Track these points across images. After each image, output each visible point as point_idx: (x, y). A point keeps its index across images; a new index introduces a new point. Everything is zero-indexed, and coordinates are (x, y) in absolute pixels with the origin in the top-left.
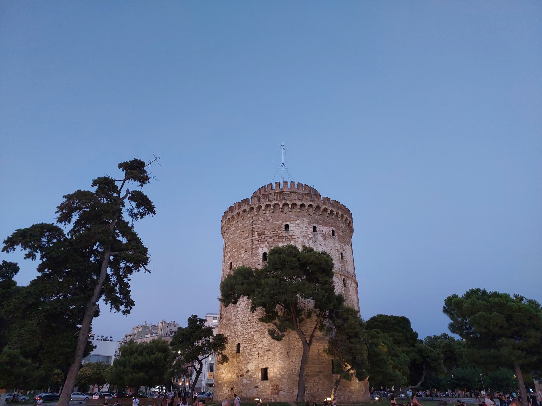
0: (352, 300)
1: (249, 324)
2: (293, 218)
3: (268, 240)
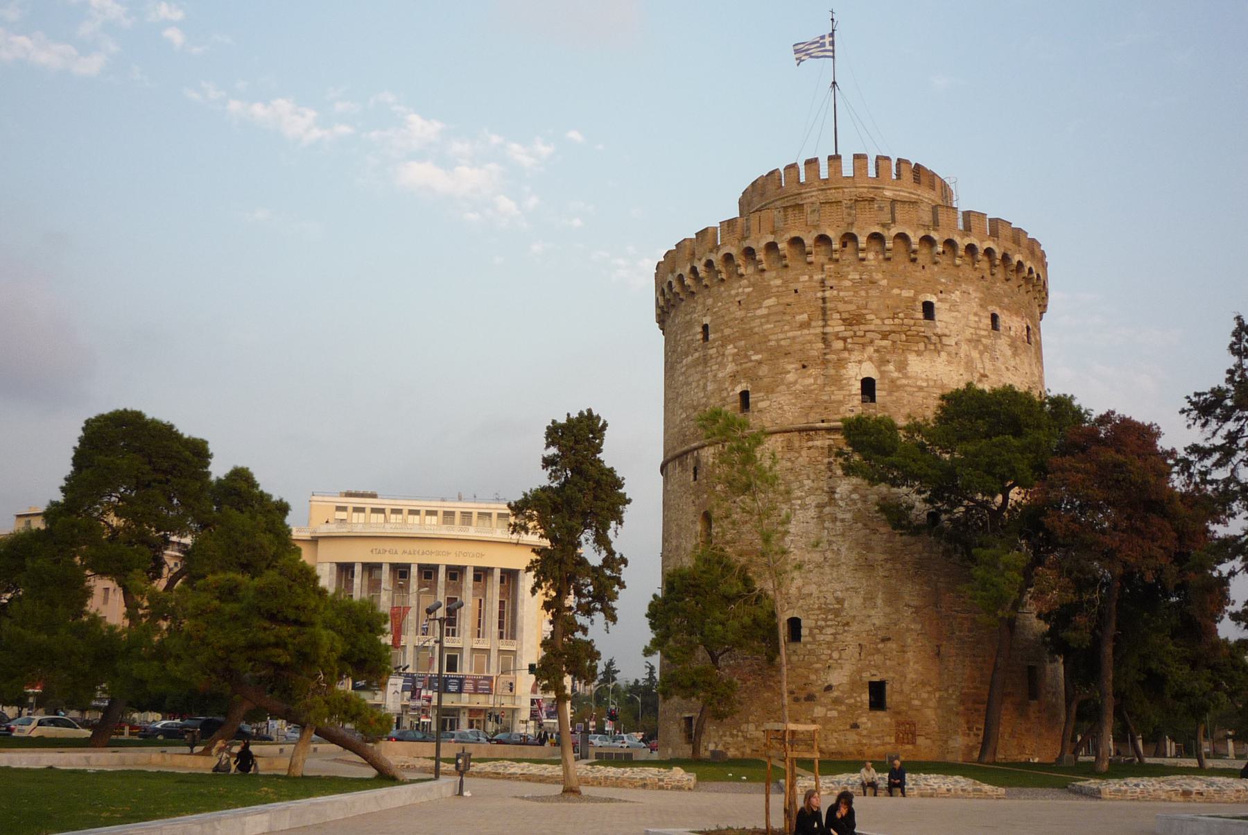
1: (827, 570)
2: (944, 284)
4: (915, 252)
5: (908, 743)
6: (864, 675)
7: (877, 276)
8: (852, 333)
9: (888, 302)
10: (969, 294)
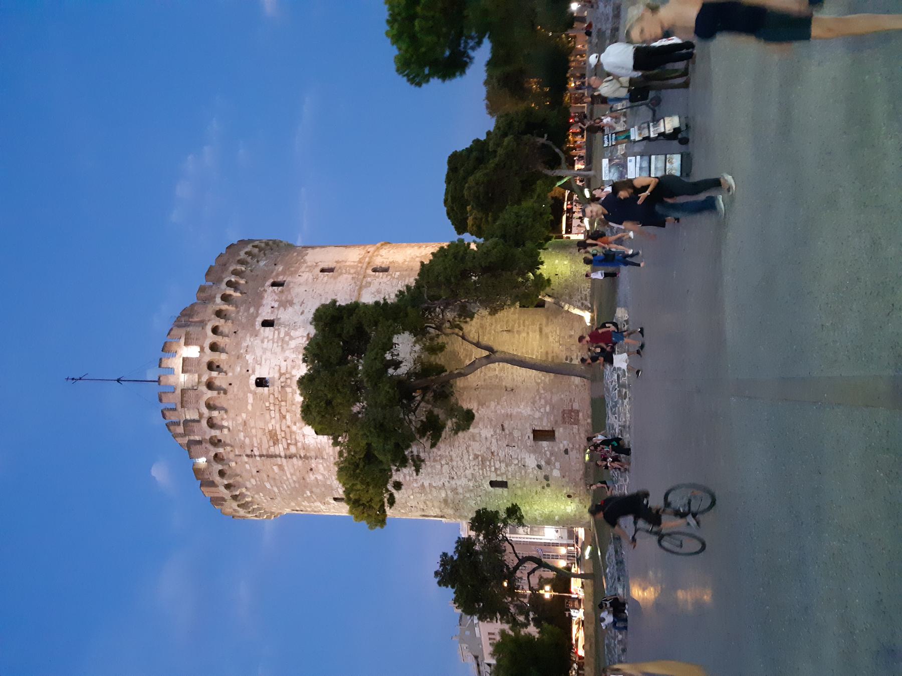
0: (414, 257)
1: (454, 463)
3: (289, 423)
4: (219, 393)
5: (578, 416)
6: (529, 444)
7: (240, 420)
8: (284, 440)
9: (258, 414)
10: (247, 346)
